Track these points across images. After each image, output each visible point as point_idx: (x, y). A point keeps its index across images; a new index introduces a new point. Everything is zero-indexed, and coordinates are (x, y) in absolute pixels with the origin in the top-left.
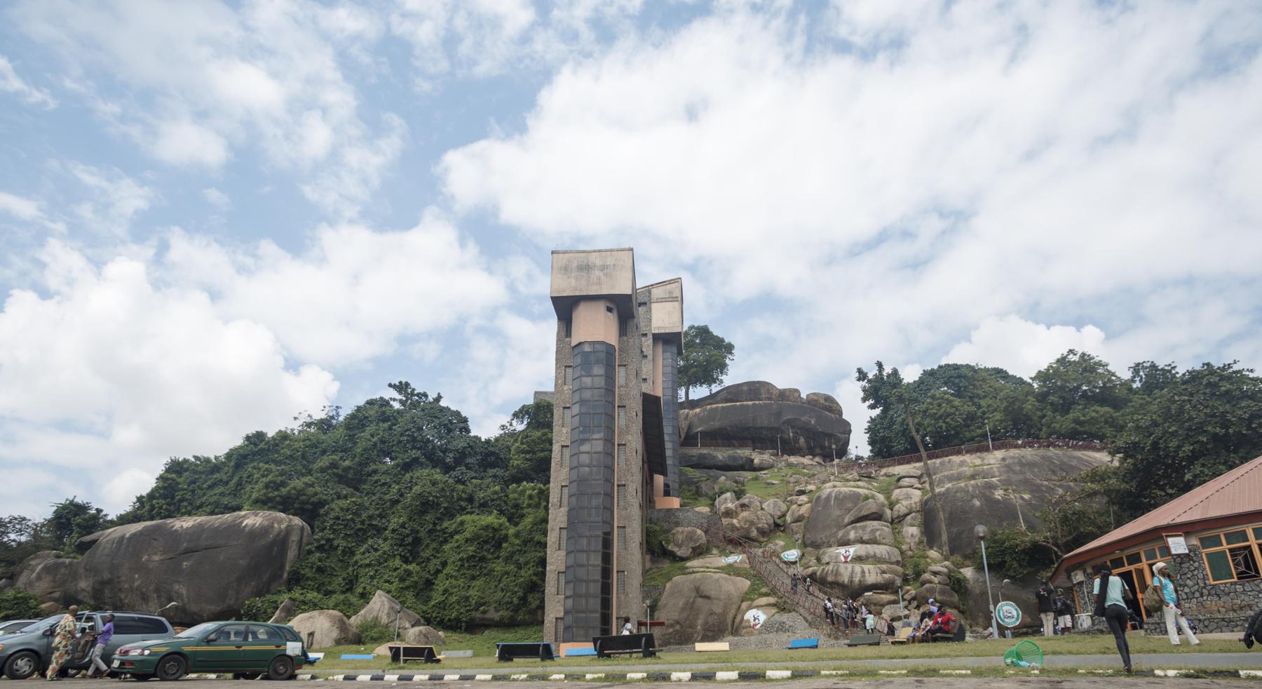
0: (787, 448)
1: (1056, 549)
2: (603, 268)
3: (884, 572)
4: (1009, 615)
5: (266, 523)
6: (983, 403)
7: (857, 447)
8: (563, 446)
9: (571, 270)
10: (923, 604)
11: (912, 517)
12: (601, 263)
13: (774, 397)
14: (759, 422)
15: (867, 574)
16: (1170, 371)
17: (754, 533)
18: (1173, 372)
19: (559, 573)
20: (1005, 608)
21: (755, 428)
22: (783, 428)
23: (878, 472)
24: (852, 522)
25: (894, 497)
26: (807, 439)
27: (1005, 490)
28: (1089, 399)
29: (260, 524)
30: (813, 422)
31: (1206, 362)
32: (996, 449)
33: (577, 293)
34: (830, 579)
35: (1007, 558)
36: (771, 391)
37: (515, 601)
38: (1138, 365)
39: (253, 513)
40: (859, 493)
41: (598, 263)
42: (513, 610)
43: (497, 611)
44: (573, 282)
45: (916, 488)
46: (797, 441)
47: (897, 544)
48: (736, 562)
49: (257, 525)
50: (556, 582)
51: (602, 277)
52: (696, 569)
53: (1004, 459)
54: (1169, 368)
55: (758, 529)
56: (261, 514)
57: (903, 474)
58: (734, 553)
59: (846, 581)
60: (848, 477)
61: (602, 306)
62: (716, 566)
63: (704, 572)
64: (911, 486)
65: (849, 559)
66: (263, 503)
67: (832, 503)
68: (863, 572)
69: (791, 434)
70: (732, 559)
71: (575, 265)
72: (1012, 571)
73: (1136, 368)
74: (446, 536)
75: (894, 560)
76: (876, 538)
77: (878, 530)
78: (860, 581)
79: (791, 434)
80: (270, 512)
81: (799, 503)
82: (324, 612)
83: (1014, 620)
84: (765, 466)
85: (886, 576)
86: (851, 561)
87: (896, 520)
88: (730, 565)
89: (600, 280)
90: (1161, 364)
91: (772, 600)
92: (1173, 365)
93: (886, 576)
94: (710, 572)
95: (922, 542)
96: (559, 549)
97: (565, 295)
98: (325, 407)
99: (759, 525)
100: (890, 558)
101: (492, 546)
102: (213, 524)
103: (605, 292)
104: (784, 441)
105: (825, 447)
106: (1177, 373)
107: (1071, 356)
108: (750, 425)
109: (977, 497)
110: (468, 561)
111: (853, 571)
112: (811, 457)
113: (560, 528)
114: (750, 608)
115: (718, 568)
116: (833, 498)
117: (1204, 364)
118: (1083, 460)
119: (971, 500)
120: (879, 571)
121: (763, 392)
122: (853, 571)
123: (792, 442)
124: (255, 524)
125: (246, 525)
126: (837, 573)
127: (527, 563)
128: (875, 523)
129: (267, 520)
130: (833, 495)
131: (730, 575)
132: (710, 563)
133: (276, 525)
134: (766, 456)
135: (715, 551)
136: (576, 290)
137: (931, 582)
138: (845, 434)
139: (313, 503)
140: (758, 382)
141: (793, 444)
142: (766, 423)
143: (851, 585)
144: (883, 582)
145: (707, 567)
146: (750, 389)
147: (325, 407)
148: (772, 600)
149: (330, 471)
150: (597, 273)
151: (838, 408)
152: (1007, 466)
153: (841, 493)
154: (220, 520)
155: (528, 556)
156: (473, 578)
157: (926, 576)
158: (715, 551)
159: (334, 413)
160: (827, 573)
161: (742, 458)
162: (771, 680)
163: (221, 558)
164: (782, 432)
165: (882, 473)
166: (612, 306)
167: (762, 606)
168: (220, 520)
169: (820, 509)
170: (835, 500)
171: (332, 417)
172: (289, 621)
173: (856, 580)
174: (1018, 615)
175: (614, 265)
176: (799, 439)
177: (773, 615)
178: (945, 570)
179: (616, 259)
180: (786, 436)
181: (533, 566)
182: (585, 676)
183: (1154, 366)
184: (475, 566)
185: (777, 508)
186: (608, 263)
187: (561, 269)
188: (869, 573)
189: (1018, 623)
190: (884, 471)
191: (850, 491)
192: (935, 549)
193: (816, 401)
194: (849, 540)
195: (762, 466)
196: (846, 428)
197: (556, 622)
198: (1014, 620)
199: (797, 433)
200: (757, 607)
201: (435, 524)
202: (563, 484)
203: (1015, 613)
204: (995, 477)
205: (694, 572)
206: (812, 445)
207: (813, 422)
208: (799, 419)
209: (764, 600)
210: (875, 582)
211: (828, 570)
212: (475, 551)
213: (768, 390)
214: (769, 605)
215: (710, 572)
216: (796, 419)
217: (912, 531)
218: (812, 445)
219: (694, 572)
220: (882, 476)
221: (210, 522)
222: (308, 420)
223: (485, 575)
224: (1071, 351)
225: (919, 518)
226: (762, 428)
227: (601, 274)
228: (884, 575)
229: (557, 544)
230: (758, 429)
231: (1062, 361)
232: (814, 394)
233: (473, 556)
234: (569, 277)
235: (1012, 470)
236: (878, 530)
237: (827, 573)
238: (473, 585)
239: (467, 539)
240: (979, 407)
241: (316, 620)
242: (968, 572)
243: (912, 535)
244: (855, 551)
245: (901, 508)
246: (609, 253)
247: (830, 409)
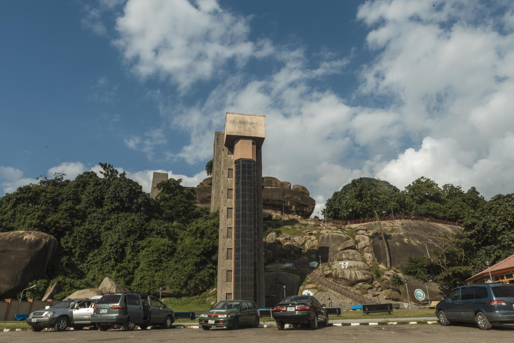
1: (443, 267)
2: (252, 124)
3: (364, 274)
4: (420, 295)
5: (37, 238)
6: (381, 196)
7: (318, 212)
8: (228, 208)
9: (236, 123)
10: (384, 289)
11: (367, 249)
12: (250, 121)
13: (278, 185)
14: (274, 197)
15: (358, 275)
16: (458, 189)
17: (293, 253)
18: (460, 190)
19: (228, 271)
20: (418, 292)
21: (272, 200)
22: (285, 201)
23: (345, 226)
24: (342, 250)
25: (356, 239)
26: (296, 207)
27: (408, 239)
28: (432, 199)
29: (34, 239)
30: (299, 199)
31: (473, 187)
32: (396, 219)
33: (240, 135)
34: (340, 276)
35: (419, 270)
36: (277, 182)
37: (182, 284)
38: (446, 185)
39: (27, 232)
40: (342, 236)
41: (249, 121)
42: (180, 288)
43: (171, 288)
44: (237, 129)
45: (365, 235)
47: (364, 260)
48: (290, 266)
49: (33, 239)
50: (226, 275)
51: (251, 128)
52: (273, 270)
53: (402, 224)
54: (458, 188)
55: (294, 251)
56: (32, 233)
57: (359, 228)
58: (286, 262)
59: (348, 278)
60: (332, 228)
61: (250, 142)
62: (281, 268)
63: (277, 271)
64: (364, 234)
65: (346, 267)
66: (32, 227)
67: (330, 240)
68: (356, 274)
70: (287, 265)
71: (238, 120)
72: (420, 275)
73: (445, 186)
74: (139, 248)
75: (366, 268)
76: (355, 258)
77: (355, 254)
78: (355, 278)
79: (289, 204)
80: (38, 232)
81: (312, 239)
82: (93, 290)
83: (422, 297)
84: (278, 219)
85: (367, 276)
86: (347, 268)
87: (360, 250)
88: (287, 268)
89: (250, 129)
90: (455, 186)
91: (313, 286)
92: (460, 187)
93: (367, 276)
94: (280, 271)
95: (375, 260)
96: (227, 259)
97: (233, 134)
98: (56, 173)
99: (295, 249)
100: (364, 268)
101: (166, 255)
102: (4, 238)
103: (253, 135)
104: (286, 208)
106: (461, 190)
107: (422, 179)
108: (270, 198)
109: (397, 241)
110: (154, 262)
111: (351, 273)
112: (297, 215)
113: (228, 249)
114: (304, 289)
115: (282, 269)
116: (330, 238)
117: (472, 187)
118: (435, 227)
119: (395, 243)
120: (362, 274)
121: (273, 182)
122: (351, 273)
124: (31, 238)
125: (26, 239)
126: (343, 274)
127: (188, 264)
128: (353, 251)
129: (38, 237)
130: (330, 236)
131: (289, 273)
132: (278, 267)
133: (43, 240)
135: (277, 261)
136: (239, 133)
137: (386, 279)
139: (62, 228)
140: (271, 178)
142: (277, 199)
143: (351, 280)
144: (365, 279)
145: (277, 269)
146: (267, 181)
147: (56, 173)
148: (313, 286)
149: (69, 211)
150: (249, 126)
151: (308, 193)
152: (405, 228)
153: (334, 236)
154: (8, 236)
155: (189, 261)
156: (156, 271)
157: (385, 277)
158: (277, 261)
159: (60, 177)
160: (338, 274)
161: (267, 214)
162: (429, 324)
163: (13, 258)
164: (285, 202)
165: (347, 227)
166: (254, 142)
167: (310, 289)
168: (8, 236)
169: (325, 243)
170: (331, 239)
171: (59, 179)
172: (70, 294)
173: (353, 276)
174: (423, 295)
175: (257, 123)
176: (292, 207)
177: (316, 293)
178: (392, 274)
179: (257, 120)
180: (286, 205)
181: (191, 266)
182: (208, 322)
183: (452, 186)
184: (157, 265)
185: (300, 241)
186: (254, 122)
187: (231, 122)
188: (358, 274)
189: (423, 299)
190: (347, 226)
191: (338, 235)
192: (382, 264)
193: (298, 189)
194: (343, 258)
195: (277, 219)
196: (313, 203)
197: (227, 296)
198: (422, 297)
199: (292, 204)
200: (308, 289)
201: (134, 242)
202: (228, 227)
203: (422, 294)
204: (401, 232)
205: (271, 271)
207: (299, 199)
209: (310, 286)
210: (362, 279)
211: (339, 272)
212: (157, 257)
213: (276, 182)
214: (313, 288)
215: (280, 271)
217: (368, 256)
219: (271, 271)
220: (347, 228)
221: (2, 236)
222: (44, 180)
223: (163, 270)
224: (422, 177)
225: (371, 249)
226: (275, 200)
227: (251, 126)
228: (366, 276)
229: (226, 256)
230: (274, 200)
231: (418, 181)
232: (297, 185)
233: (157, 260)
234: (235, 126)
235: (408, 230)
236: (355, 254)
237: (338, 274)
238: (156, 275)
239: (153, 251)
240: (379, 198)
241: (88, 294)
242: (400, 275)
243: (369, 257)
244: (348, 264)
245: (361, 244)
246: (254, 116)
247: (304, 193)
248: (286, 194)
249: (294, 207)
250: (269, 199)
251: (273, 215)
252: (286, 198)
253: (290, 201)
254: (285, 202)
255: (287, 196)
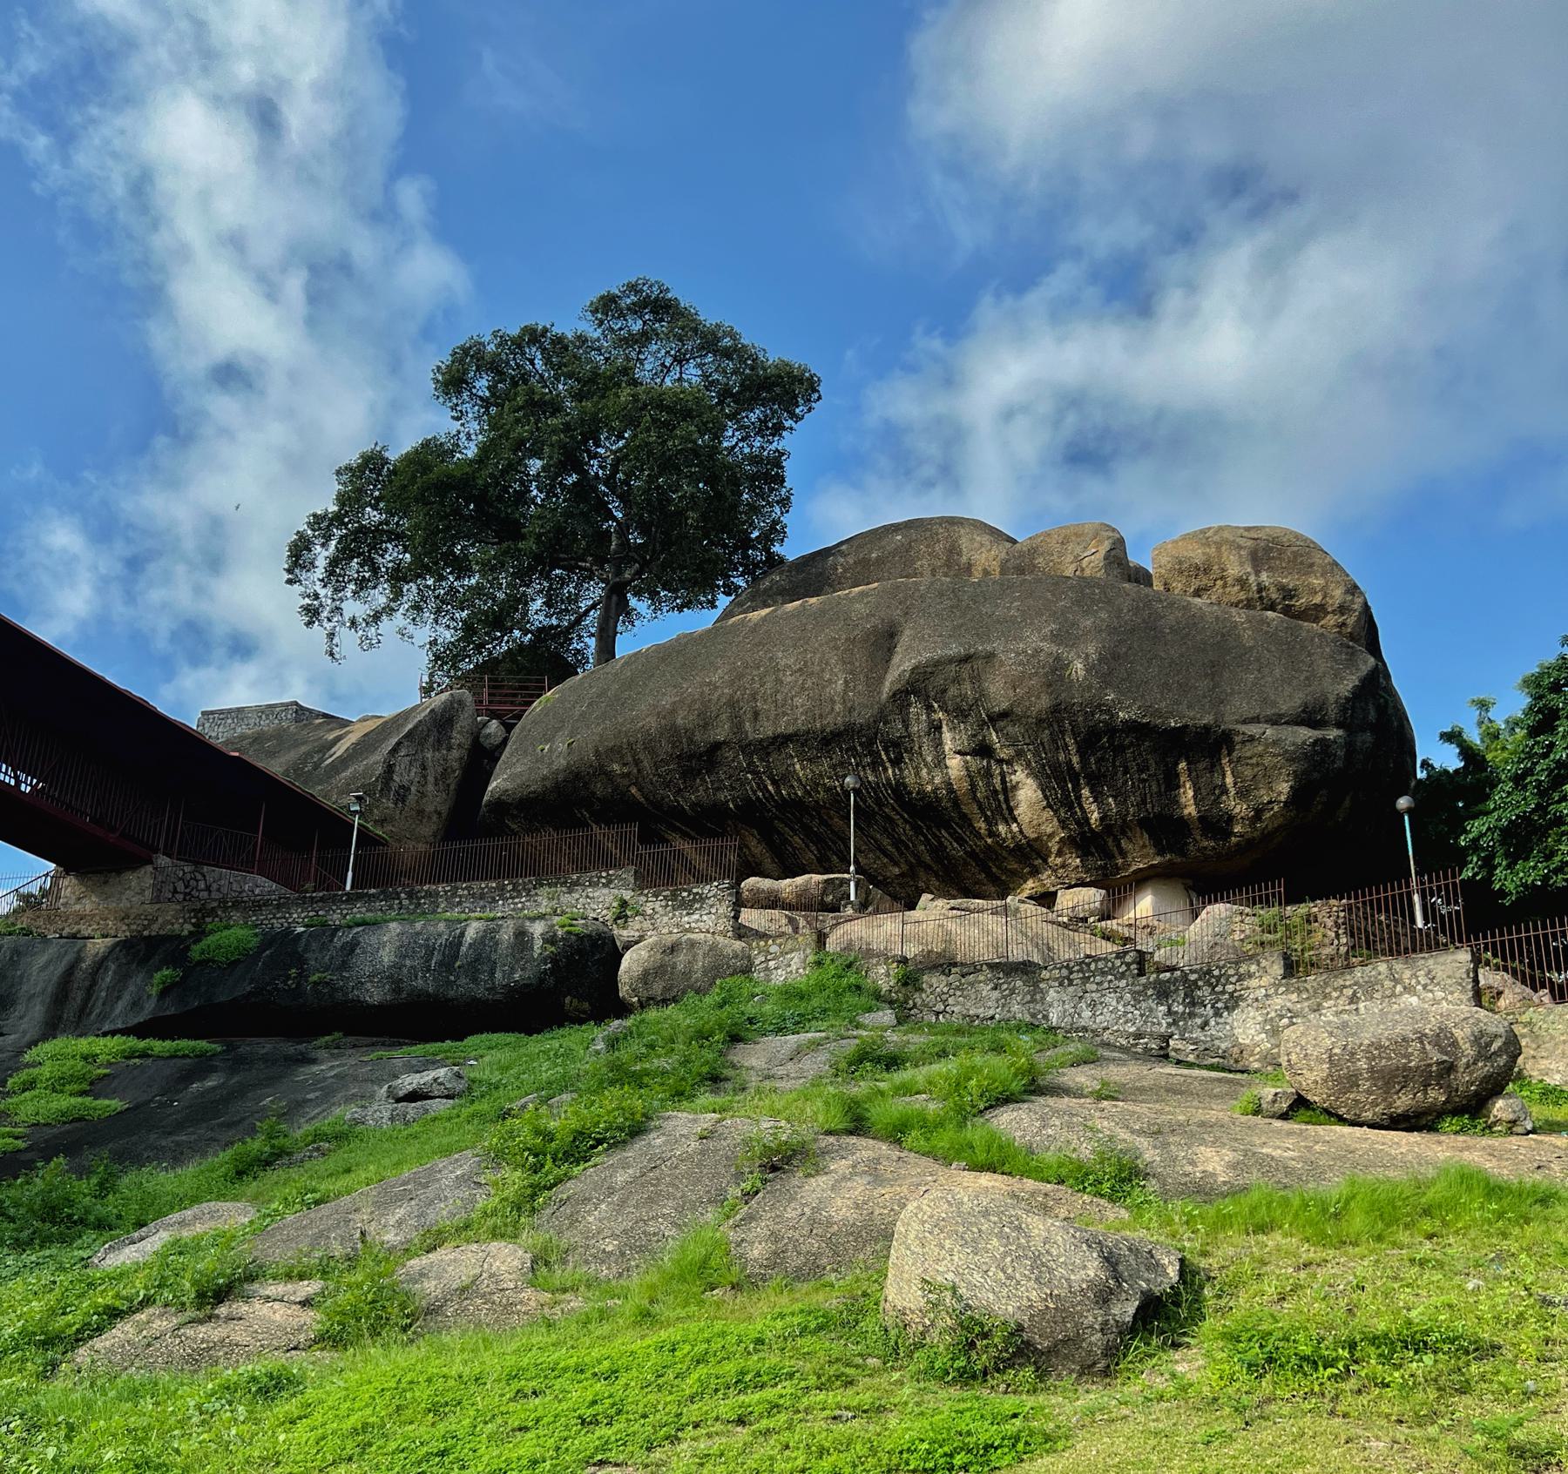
0: (956, 850)
21: (748, 748)
30: (1079, 666)
46: (1001, 804)
69: (955, 764)
79: (955, 764)
105: (1183, 822)
108: (721, 733)
112: (1091, 897)
123: (971, 809)
134: (709, 921)
138: (1314, 725)
141: (981, 825)
176: (1008, 790)
180: (924, 778)
206: (1095, 816)
208: (990, 657)
213: (953, 550)
216: (967, 659)
218: (1095, 816)
226: (781, 741)
248: (905, 639)
249: (1027, 792)
250: (717, 746)
251: (628, 946)
252: (901, 697)
253: (960, 713)
254: (899, 750)
255: (908, 666)
